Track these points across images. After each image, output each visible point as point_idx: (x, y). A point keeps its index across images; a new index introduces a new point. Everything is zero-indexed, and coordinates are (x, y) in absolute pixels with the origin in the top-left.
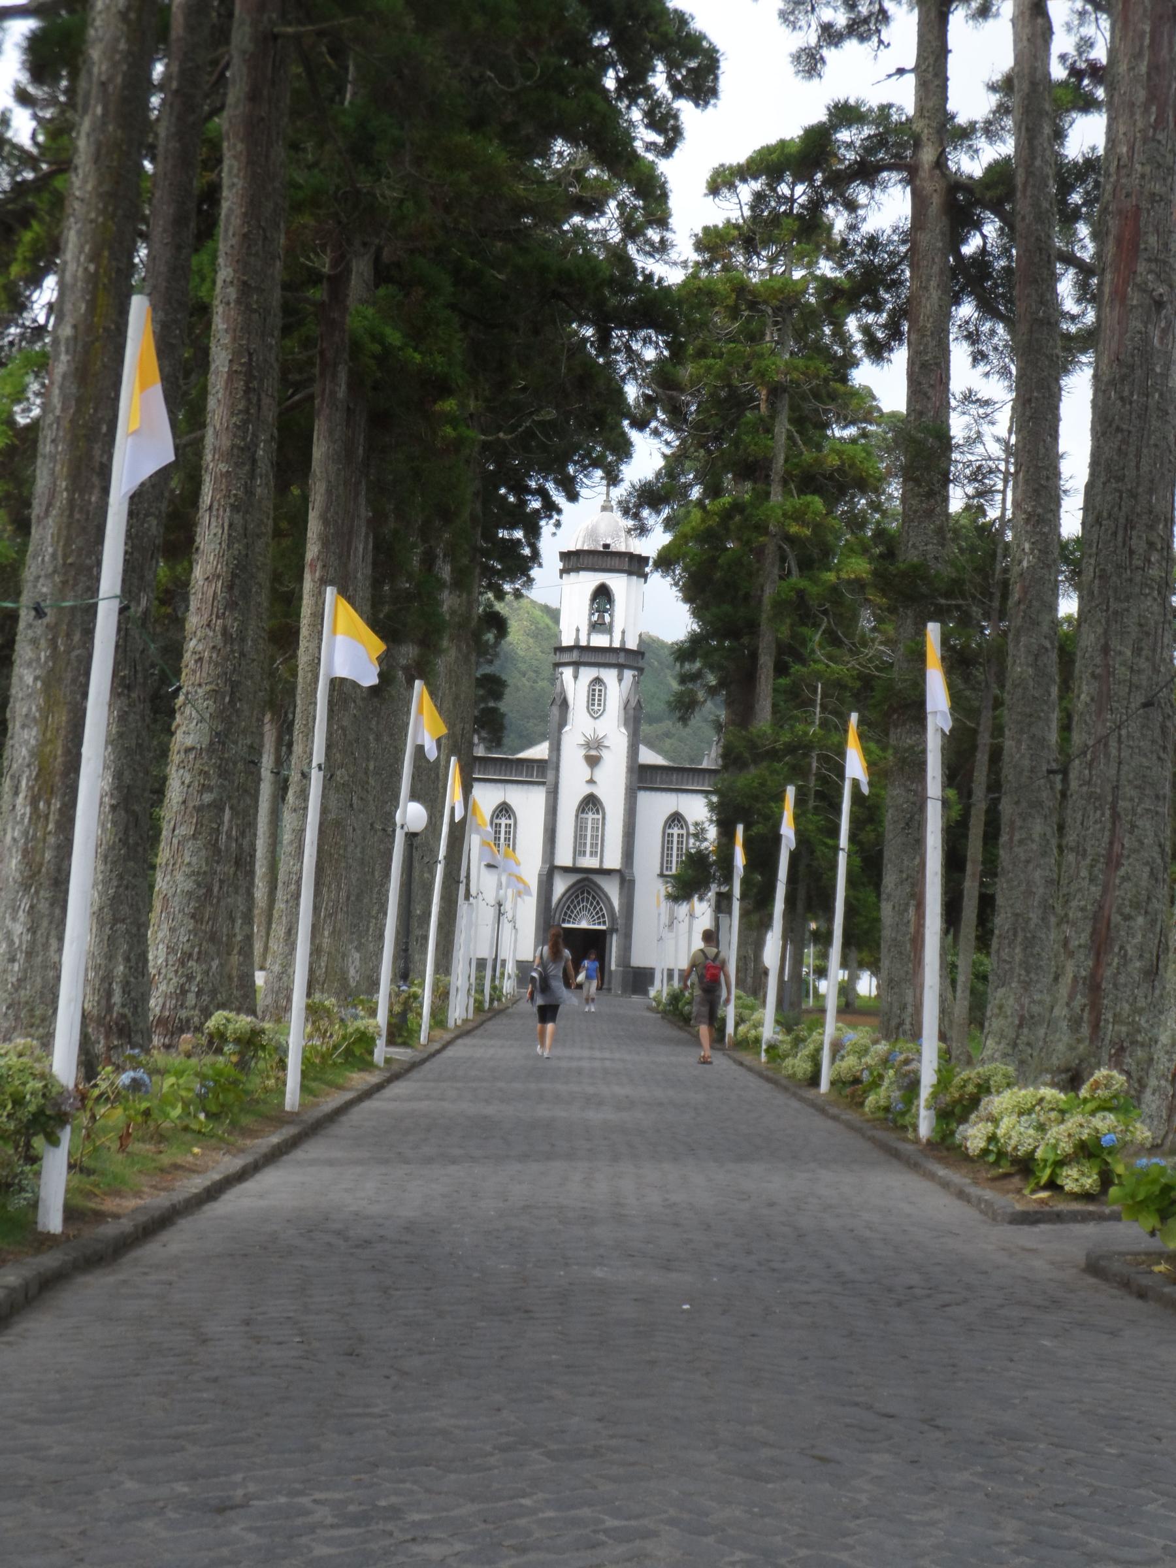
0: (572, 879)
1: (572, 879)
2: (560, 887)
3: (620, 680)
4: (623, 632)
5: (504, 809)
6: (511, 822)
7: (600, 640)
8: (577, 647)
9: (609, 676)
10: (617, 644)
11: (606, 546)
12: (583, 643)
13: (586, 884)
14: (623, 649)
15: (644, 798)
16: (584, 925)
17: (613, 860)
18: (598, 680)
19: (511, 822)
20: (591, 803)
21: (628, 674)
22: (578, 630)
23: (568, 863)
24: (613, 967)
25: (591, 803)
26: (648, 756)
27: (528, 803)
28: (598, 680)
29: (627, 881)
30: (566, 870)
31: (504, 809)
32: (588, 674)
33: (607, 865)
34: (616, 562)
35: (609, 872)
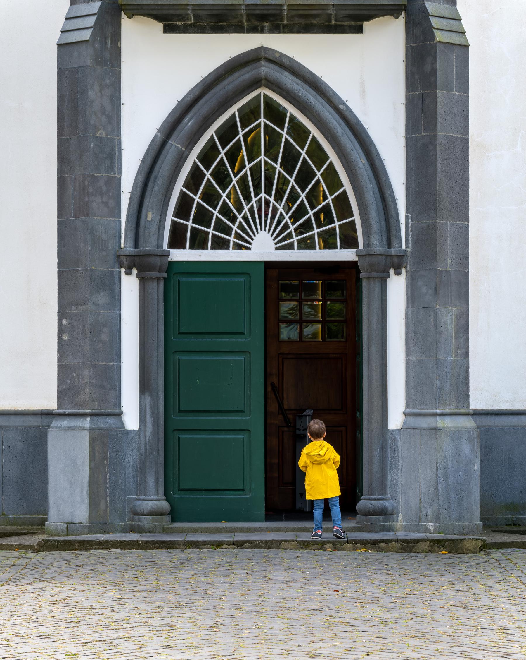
16: (263, 248)
24: (396, 420)
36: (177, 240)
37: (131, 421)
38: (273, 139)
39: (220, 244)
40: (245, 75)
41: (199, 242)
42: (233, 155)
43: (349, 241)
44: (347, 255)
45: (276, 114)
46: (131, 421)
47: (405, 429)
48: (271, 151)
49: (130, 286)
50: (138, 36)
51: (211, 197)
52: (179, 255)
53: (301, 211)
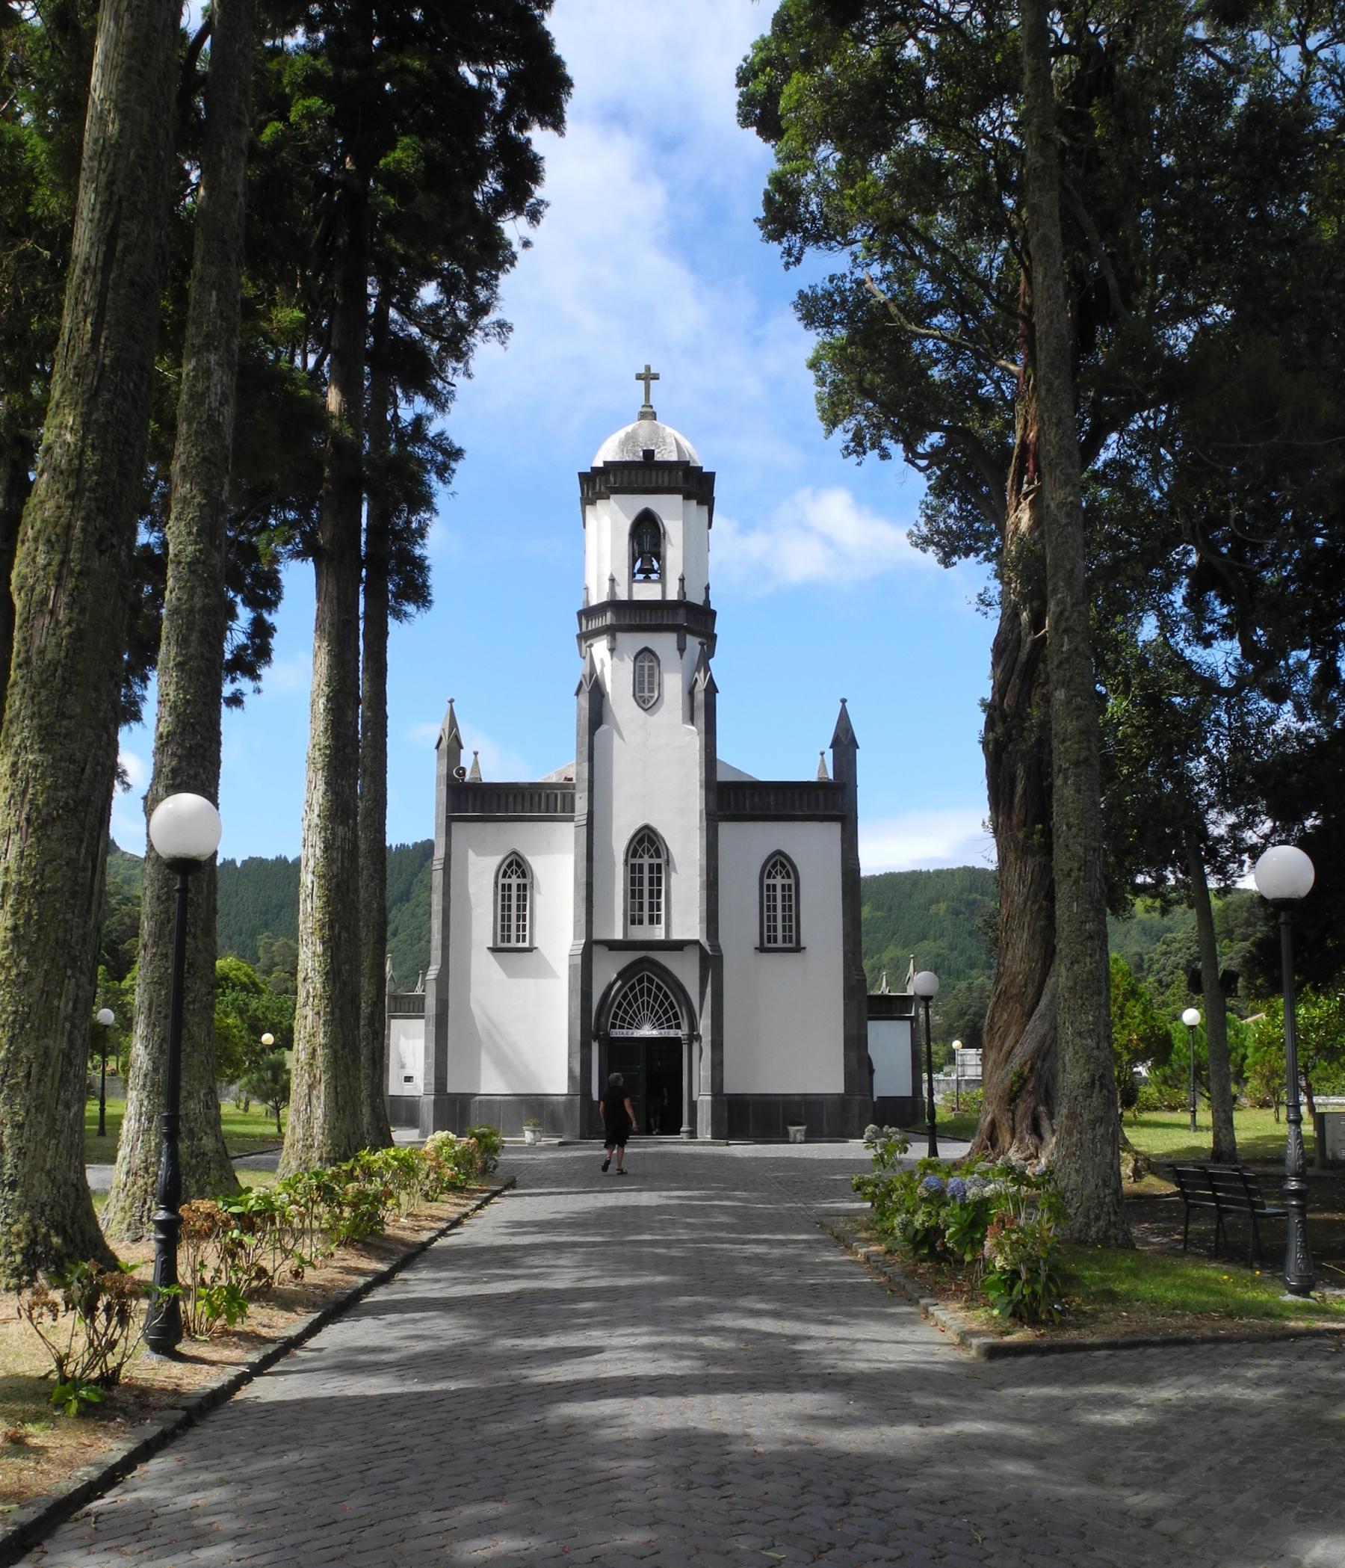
0: (627, 958)
1: (627, 958)
3: (682, 649)
4: (682, 580)
7: (646, 592)
8: (613, 605)
9: (664, 644)
10: (673, 595)
12: (623, 595)
14: (682, 604)
15: (728, 831)
16: (647, 1031)
18: (646, 652)
20: (647, 841)
21: (693, 643)
22: (612, 580)
25: (647, 841)
28: (646, 652)
29: (711, 962)
30: (613, 946)
33: (676, 936)
34: (664, 479)
35: (679, 946)
38: (650, 990)
42: (635, 997)
45: (651, 981)
46: (595, 1097)
48: (649, 996)
49: (595, 1047)
50: (598, 952)
51: (626, 1012)
52: (616, 1033)
53: (660, 1018)
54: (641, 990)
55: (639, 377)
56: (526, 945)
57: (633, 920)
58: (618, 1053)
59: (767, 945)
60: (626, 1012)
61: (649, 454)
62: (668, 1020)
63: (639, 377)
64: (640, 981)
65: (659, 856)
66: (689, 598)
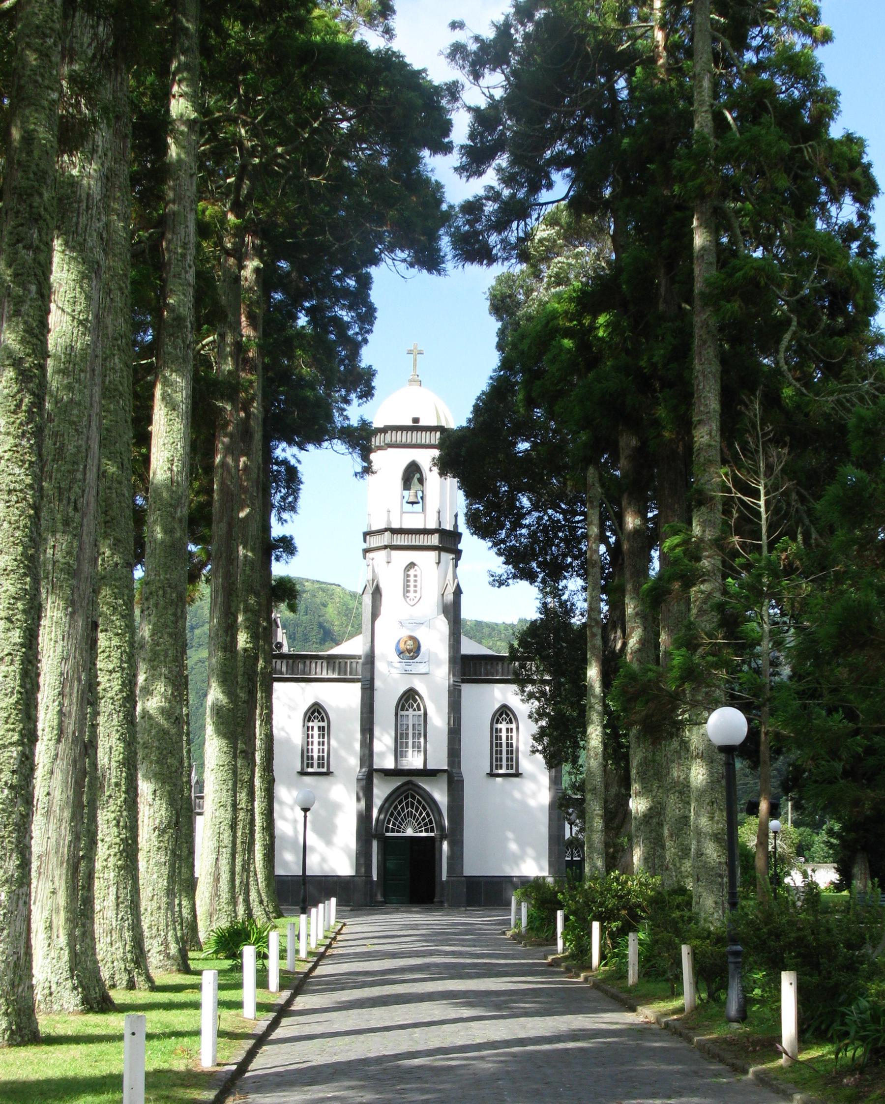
0: (397, 782)
1: (397, 782)
2: (381, 792)
5: (316, 712)
6: (325, 724)
11: (416, 420)
13: (408, 787)
15: (469, 691)
16: (409, 832)
17: (439, 760)
19: (325, 724)
23: (389, 763)
24: (444, 878)
26: (469, 647)
27: (343, 698)
30: (387, 773)
31: (316, 712)
32: (402, 558)
36: (387, 831)
37: (375, 879)
38: (413, 804)
39: (398, 832)
40: (406, 788)
41: (393, 831)
42: (402, 808)
43: (432, 831)
44: (432, 834)
46: (375, 879)
47: (447, 881)
49: (375, 844)
51: (396, 819)
52: (388, 834)
54: (407, 804)
55: (410, 352)
56: (325, 770)
57: (399, 752)
58: (390, 846)
59: (495, 772)
60: (396, 819)
61: (416, 420)
62: (426, 825)
63: (410, 352)
64: (406, 798)
65: (419, 710)
66: (443, 527)
